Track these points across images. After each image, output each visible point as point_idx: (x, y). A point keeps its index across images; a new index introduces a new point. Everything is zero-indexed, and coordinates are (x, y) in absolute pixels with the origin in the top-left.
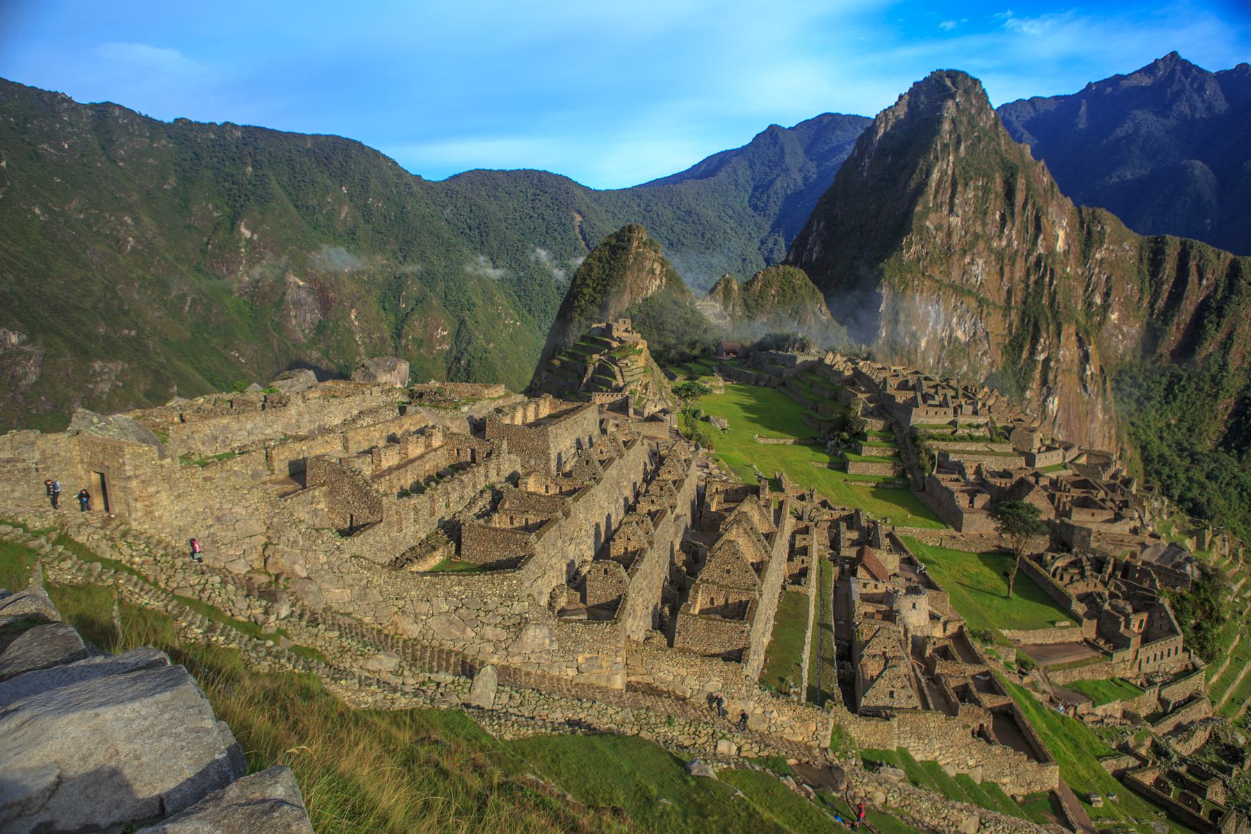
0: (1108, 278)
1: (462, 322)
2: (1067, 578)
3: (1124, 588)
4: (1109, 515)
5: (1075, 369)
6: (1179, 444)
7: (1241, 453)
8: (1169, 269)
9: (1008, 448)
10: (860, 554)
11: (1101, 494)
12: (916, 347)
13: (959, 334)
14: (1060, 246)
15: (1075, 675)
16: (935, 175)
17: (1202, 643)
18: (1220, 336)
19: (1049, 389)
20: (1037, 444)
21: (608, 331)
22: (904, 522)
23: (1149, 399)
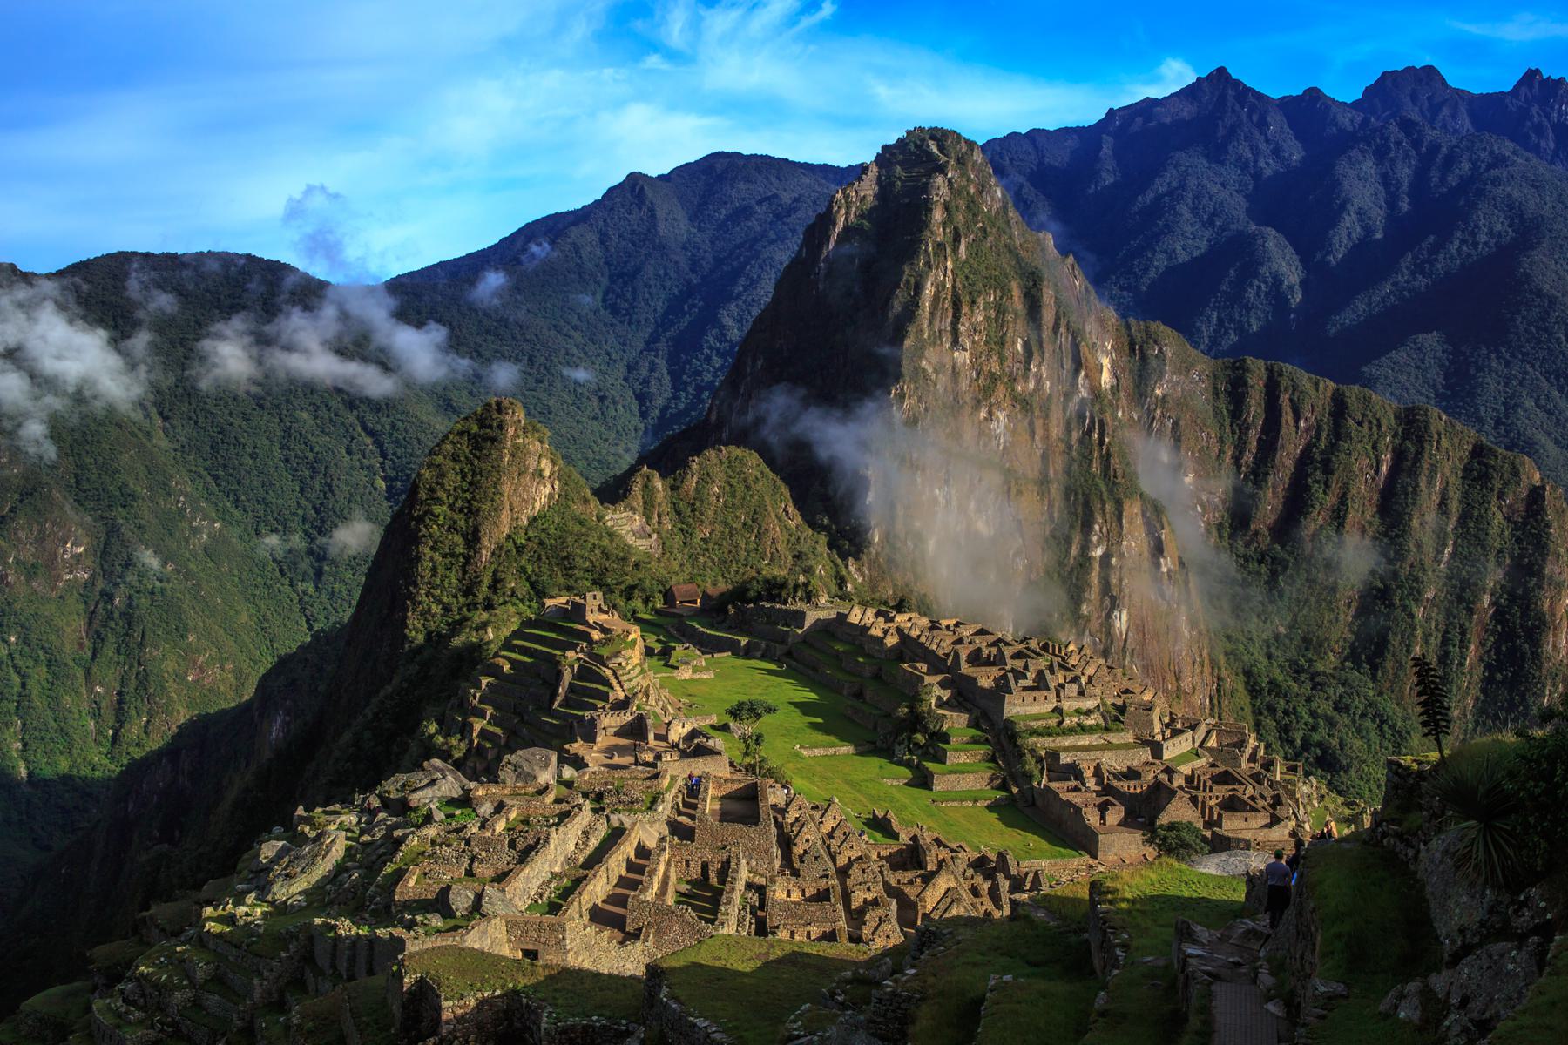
1: (113, 530)
4: (1263, 819)
7: (1374, 668)
8: (1255, 407)
9: (1129, 737)
13: (981, 526)
14: (1106, 378)
16: (929, 291)
18: (1330, 500)
19: (1113, 599)
20: (1157, 727)
21: (577, 612)
22: (1029, 854)
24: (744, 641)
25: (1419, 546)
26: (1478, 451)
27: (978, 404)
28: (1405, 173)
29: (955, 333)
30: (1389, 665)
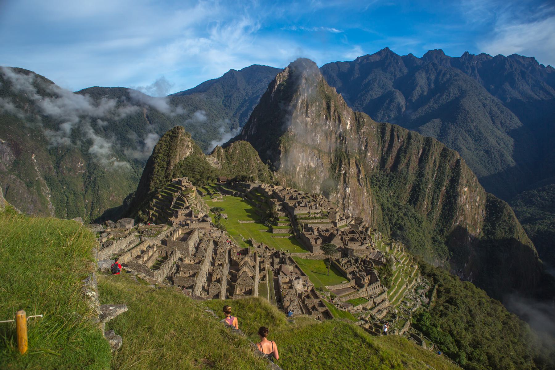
0: (366, 139)
2: (346, 266)
3: (364, 268)
4: (359, 243)
5: (356, 176)
6: (394, 203)
7: (415, 205)
8: (388, 136)
10: (281, 267)
11: (358, 236)
12: (295, 171)
13: (312, 164)
14: (348, 127)
15: (349, 298)
16: (300, 101)
17: (386, 283)
18: (406, 161)
19: (347, 185)
20: (338, 218)
21: (179, 182)
22: (294, 251)
23: (383, 186)
24: (234, 192)
25: (428, 173)
26: (444, 150)
27: (312, 131)
28: (433, 77)
29: (307, 113)
30: (418, 204)
